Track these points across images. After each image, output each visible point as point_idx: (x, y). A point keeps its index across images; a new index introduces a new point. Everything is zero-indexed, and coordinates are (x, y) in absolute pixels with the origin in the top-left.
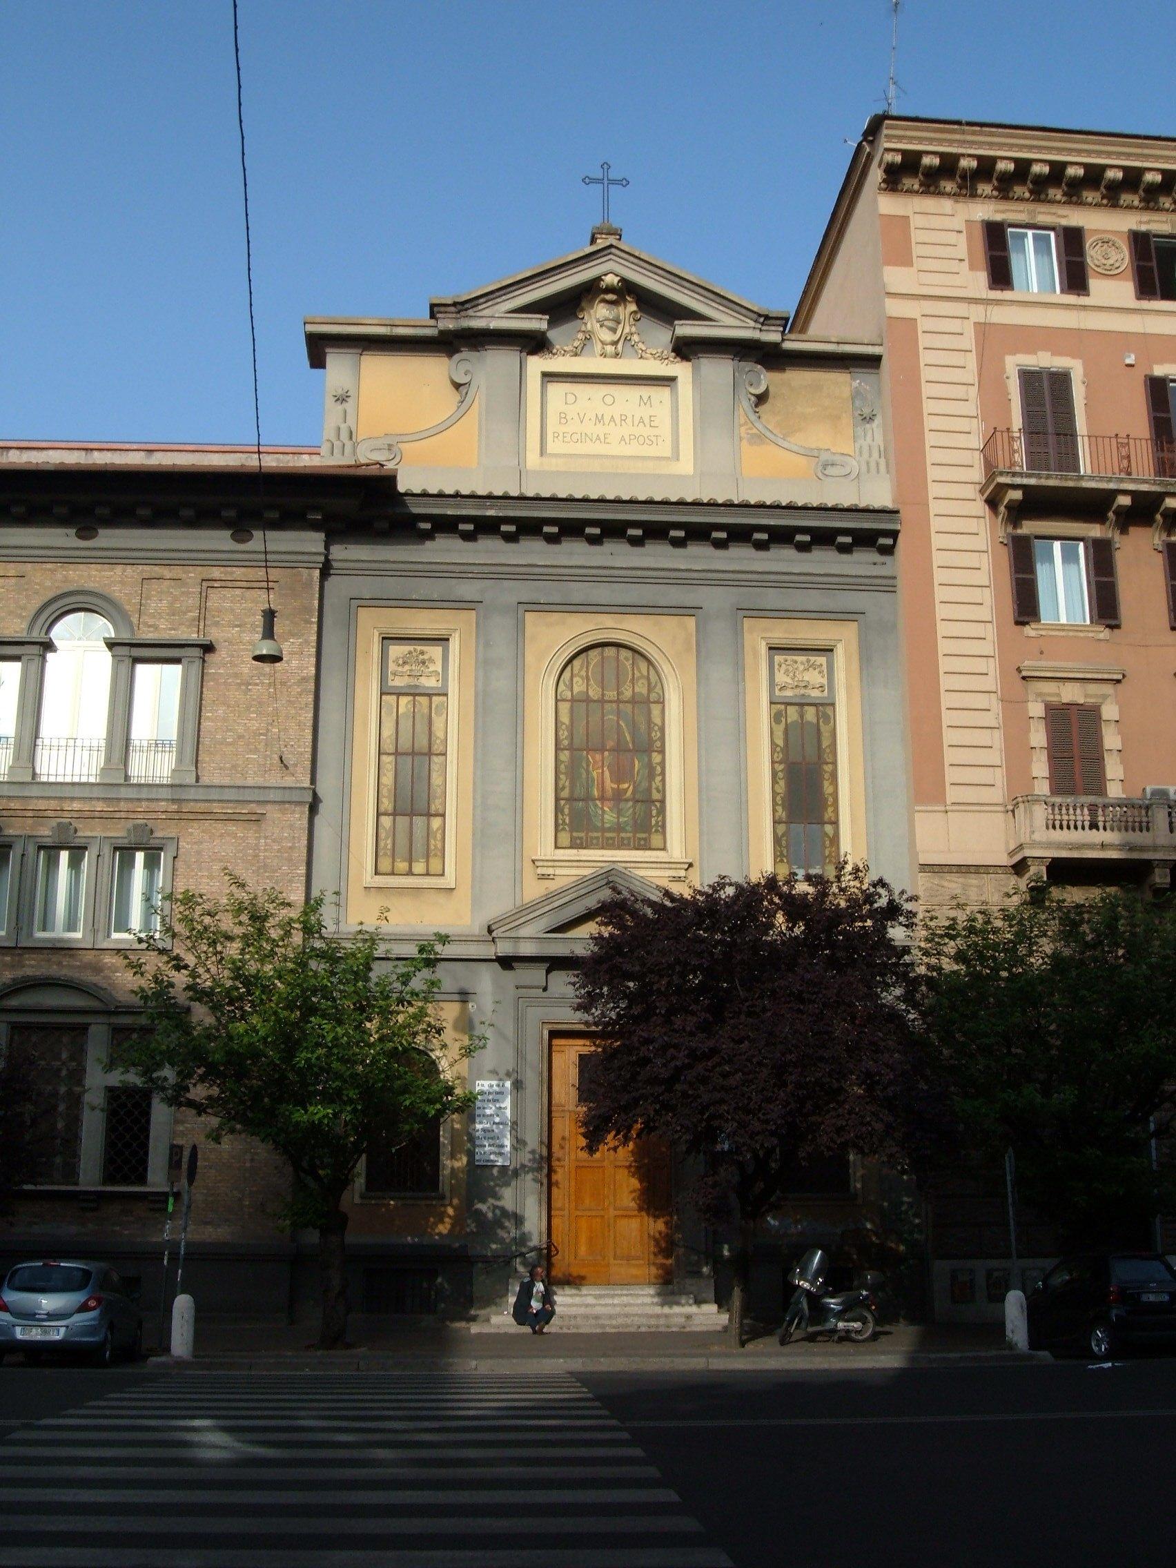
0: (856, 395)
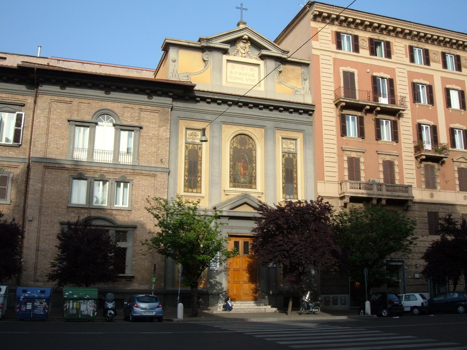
0: (302, 73)
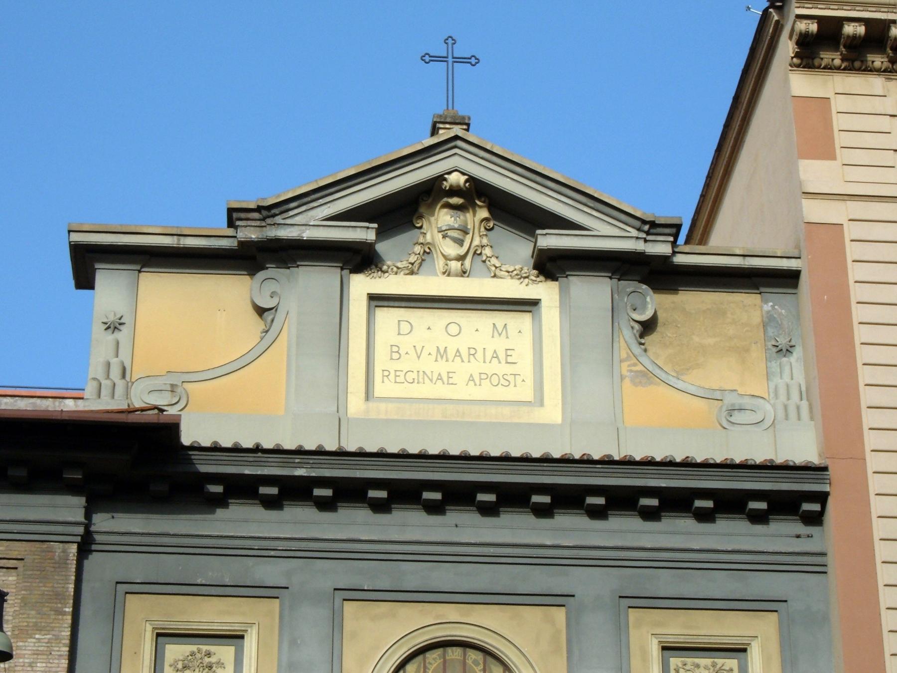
0: (768, 321)
